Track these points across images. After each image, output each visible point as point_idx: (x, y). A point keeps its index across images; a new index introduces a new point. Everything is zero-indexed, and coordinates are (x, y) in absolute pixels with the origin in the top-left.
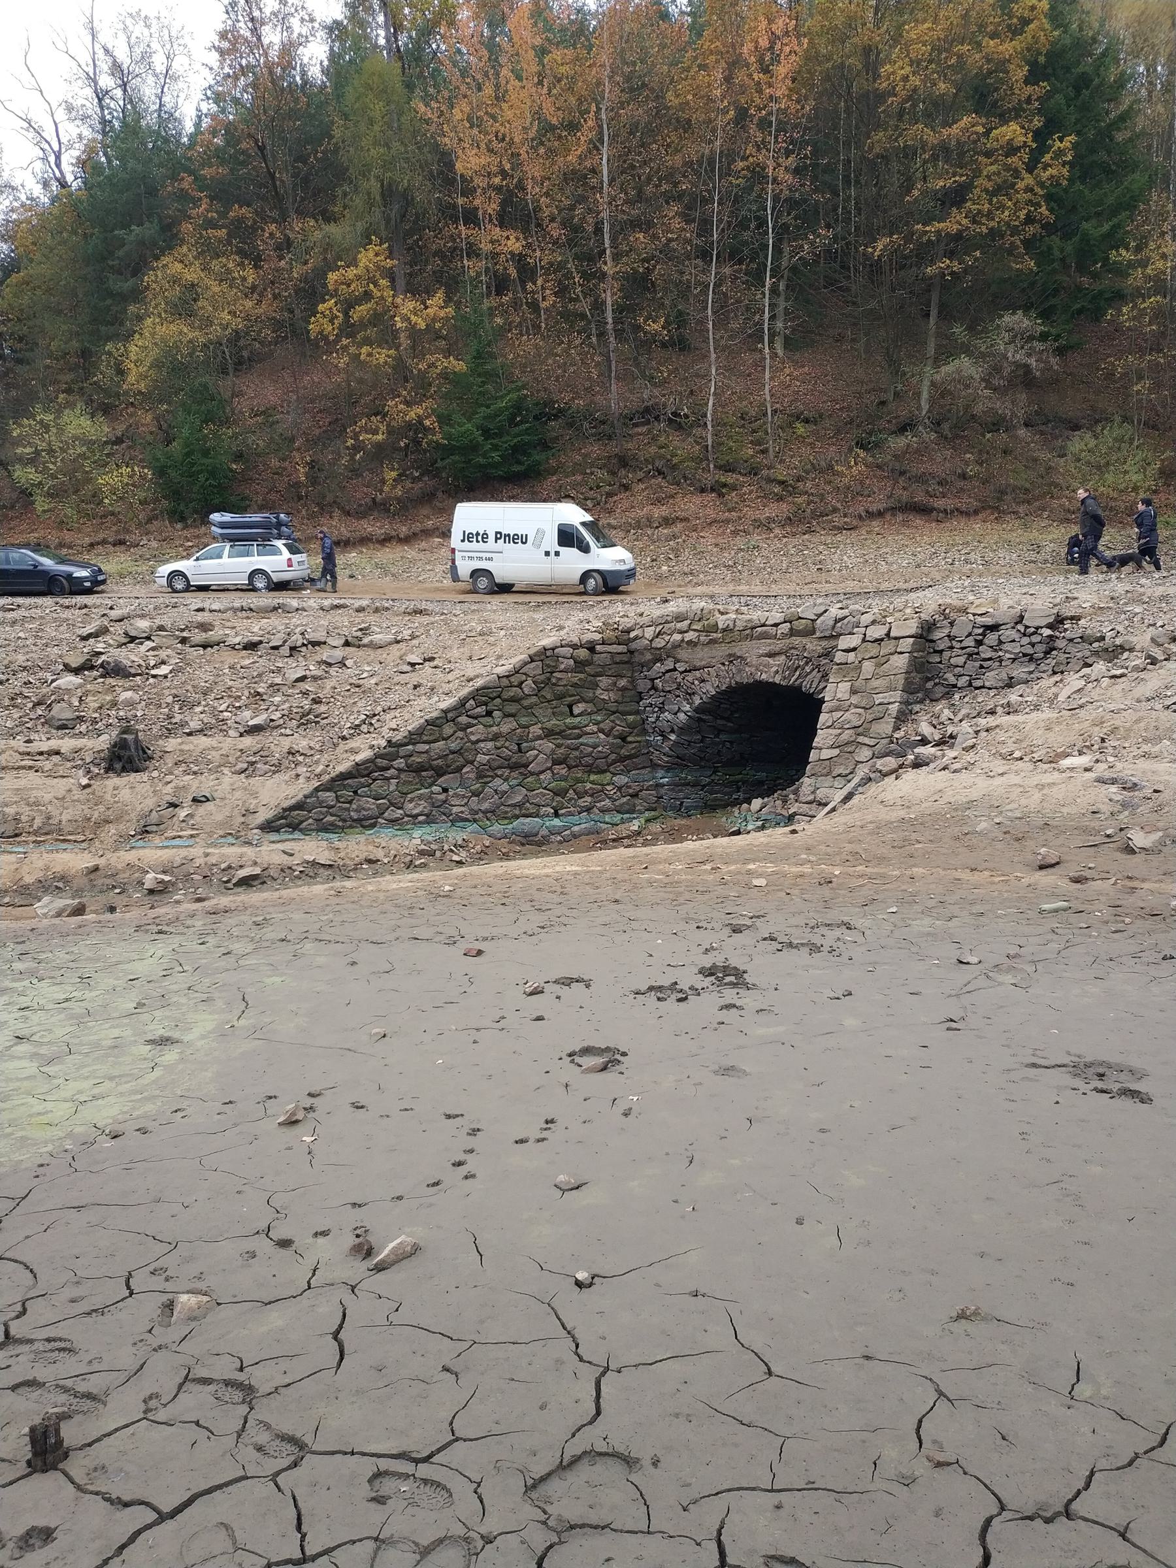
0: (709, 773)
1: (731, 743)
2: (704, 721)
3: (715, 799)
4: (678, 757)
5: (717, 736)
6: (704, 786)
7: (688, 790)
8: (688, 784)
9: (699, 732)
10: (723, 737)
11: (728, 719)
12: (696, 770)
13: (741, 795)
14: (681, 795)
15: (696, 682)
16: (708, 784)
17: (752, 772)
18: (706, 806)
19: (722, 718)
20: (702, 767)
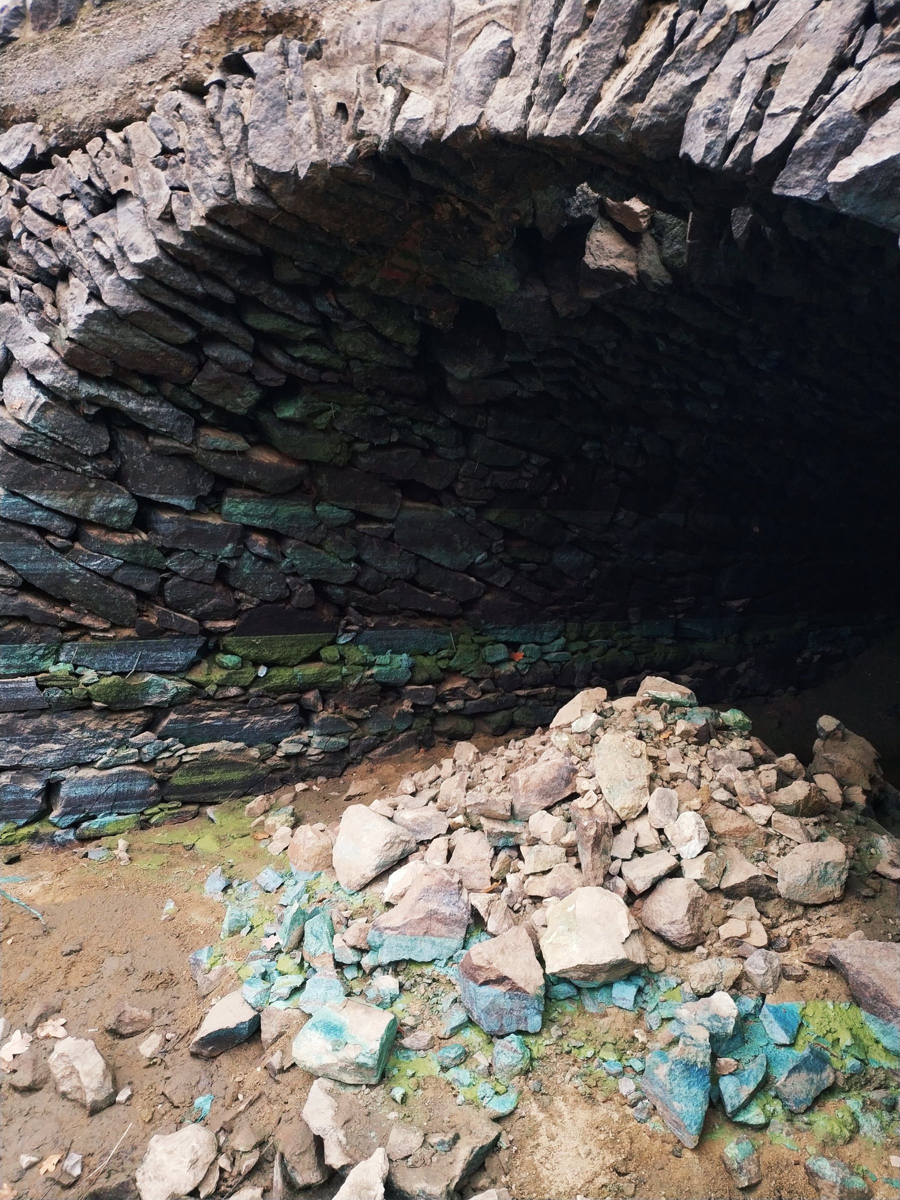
0: (178, 657)
1: (276, 536)
2: (139, 427)
3: (205, 764)
4: (26, 587)
5: (210, 502)
6: (156, 713)
7: (76, 730)
8: (84, 704)
9: (117, 477)
10: (238, 508)
11: (250, 426)
12: (121, 647)
13: (313, 741)
14: (50, 751)
15: (74, 211)
16: (176, 702)
17: (357, 654)
18: (164, 791)
19: (228, 422)
20: (148, 633)
